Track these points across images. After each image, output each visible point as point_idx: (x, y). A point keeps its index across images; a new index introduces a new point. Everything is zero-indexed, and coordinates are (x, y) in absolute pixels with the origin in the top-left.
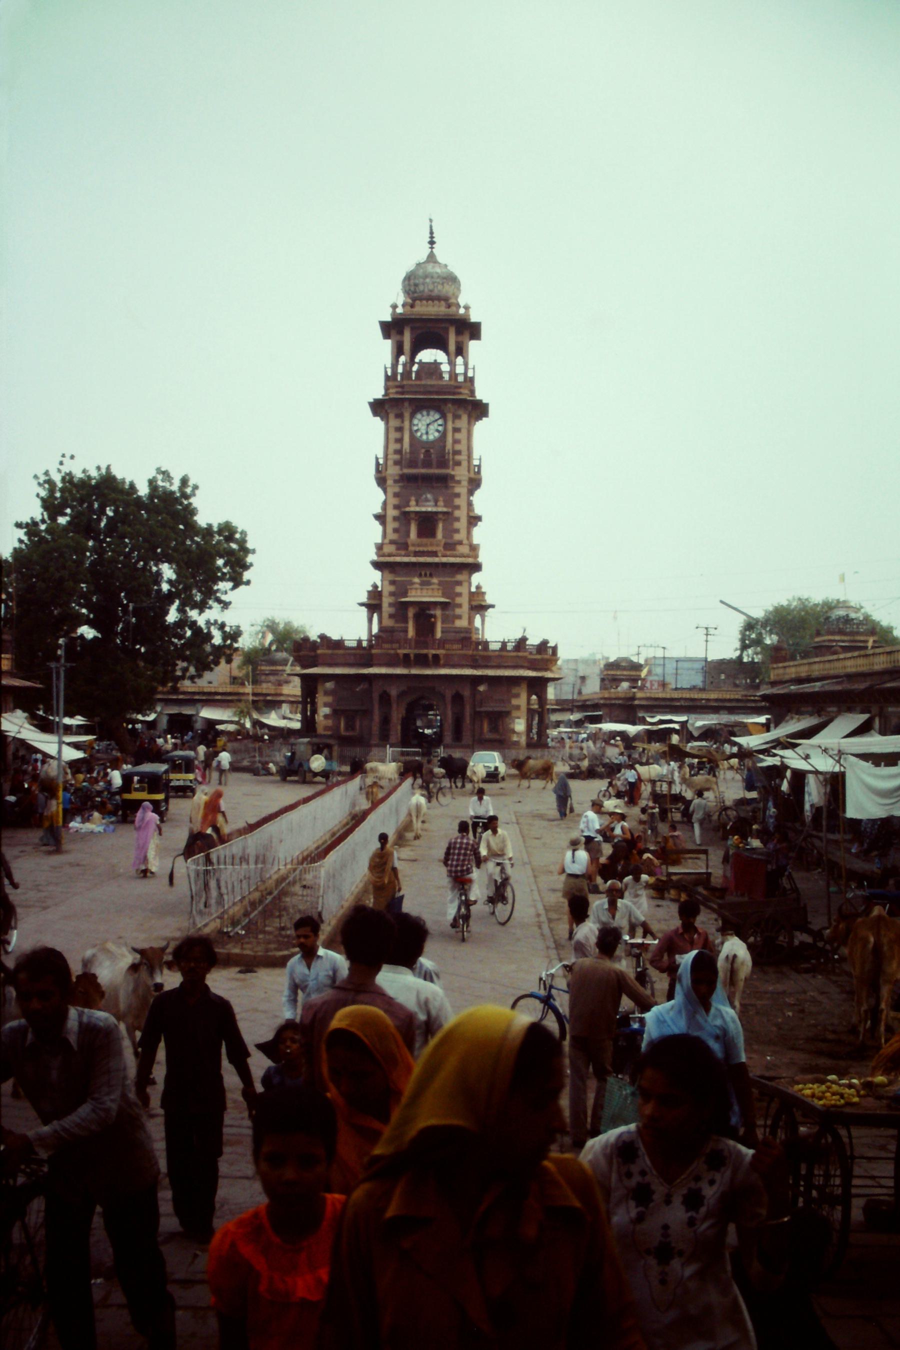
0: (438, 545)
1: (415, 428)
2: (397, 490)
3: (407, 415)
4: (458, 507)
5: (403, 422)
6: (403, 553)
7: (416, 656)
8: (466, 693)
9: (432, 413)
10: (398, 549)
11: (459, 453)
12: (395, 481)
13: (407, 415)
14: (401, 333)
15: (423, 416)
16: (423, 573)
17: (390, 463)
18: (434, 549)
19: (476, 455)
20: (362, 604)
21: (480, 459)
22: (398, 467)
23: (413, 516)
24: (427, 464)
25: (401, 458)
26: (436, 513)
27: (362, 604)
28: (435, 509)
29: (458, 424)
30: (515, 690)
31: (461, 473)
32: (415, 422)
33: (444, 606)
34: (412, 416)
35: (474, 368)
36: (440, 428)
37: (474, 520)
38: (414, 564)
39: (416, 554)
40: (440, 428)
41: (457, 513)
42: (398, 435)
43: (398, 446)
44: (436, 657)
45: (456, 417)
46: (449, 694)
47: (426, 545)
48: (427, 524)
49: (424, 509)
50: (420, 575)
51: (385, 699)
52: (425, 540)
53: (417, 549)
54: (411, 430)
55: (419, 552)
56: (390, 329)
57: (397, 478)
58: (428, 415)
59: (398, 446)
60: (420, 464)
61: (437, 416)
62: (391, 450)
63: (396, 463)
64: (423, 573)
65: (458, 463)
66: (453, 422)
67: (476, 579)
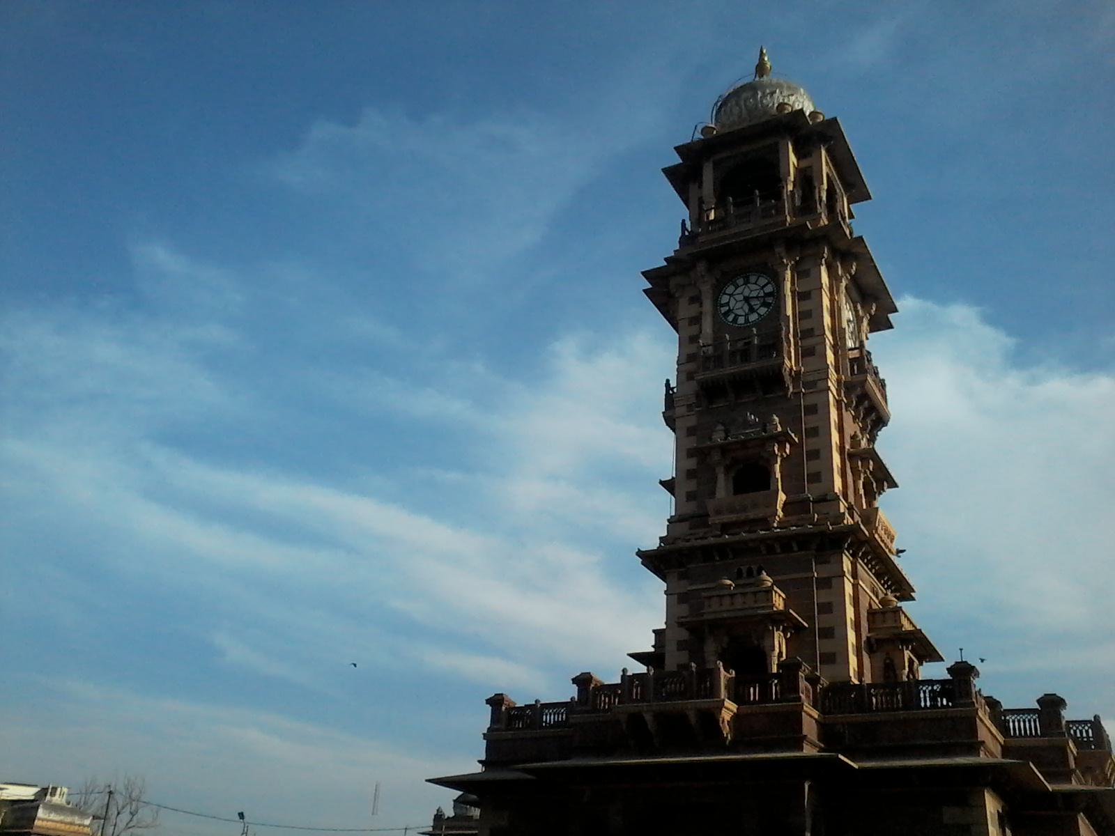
1: (724, 310)
3: (706, 289)
12: (690, 407)
15: (737, 287)
16: (744, 569)
23: (716, 456)
32: (725, 299)
34: (718, 291)
36: (770, 300)
38: (722, 550)
40: (770, 300)
47: (744, 509)
50: (739, 575)
54: (715, 315)
61: (763, 281)
64: (744, 569)
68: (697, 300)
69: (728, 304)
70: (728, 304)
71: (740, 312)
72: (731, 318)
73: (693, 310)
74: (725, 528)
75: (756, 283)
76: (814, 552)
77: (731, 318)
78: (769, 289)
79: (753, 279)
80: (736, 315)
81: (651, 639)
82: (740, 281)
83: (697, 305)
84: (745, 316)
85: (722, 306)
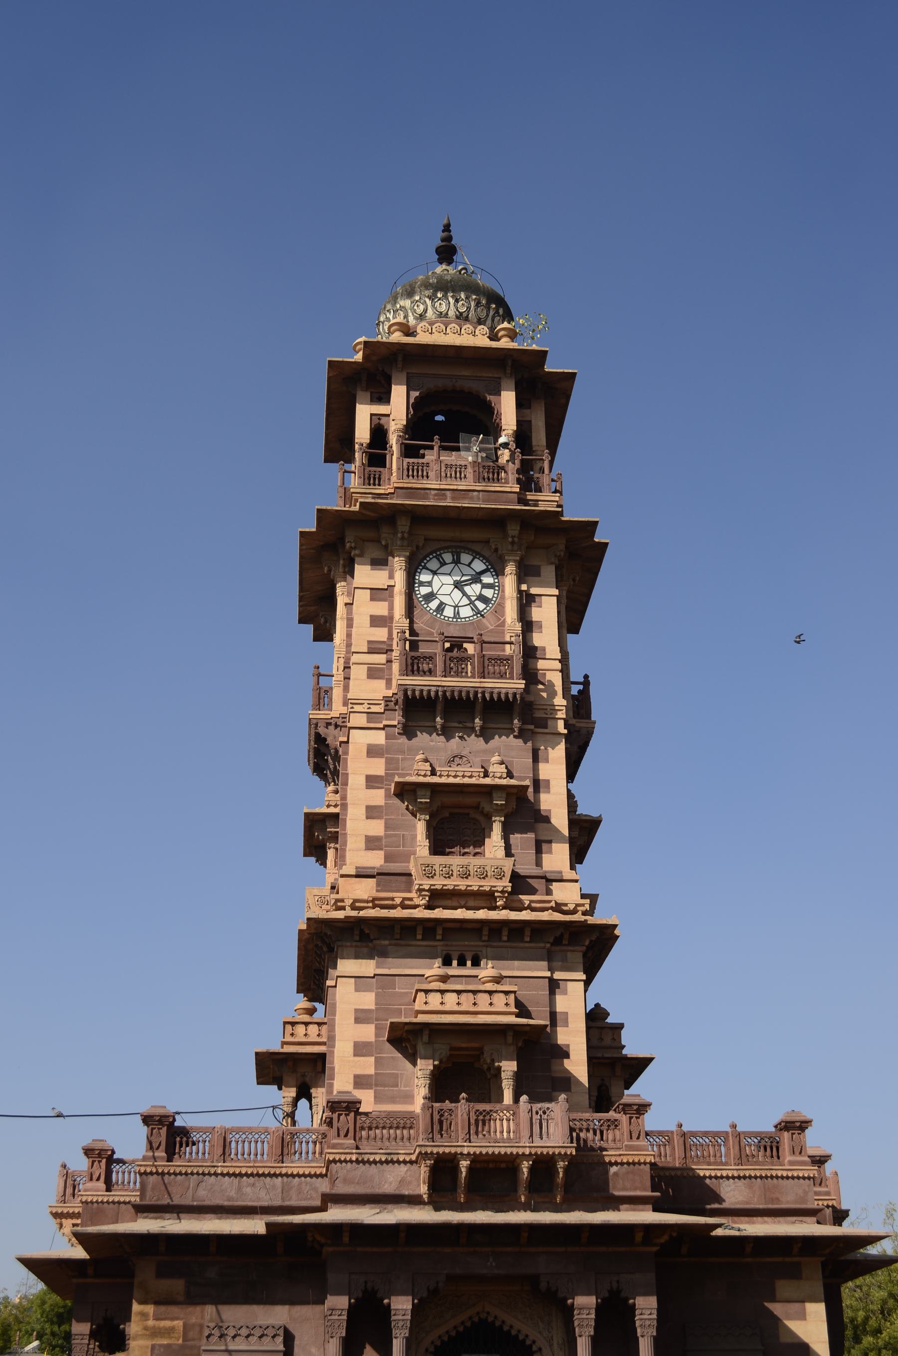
1: (424, 590)
2: (379, 738)
5: (391, 577)
6: (398, 896)
9: (465, 558)
10: (380, 887)
14: (383, 397)
15: (443, 564)
17: (358, 673)
18: (486, 885)
19: (576, 675)
21: (586, 682)
22: (380, 684)
25: (389, 661)
37: (583, 832)
38: (430, 927)
40: (488, 593)
42: (381, 609)
44: (543, 1165)
52: (455, 861)
53: (439, 883)
57: (379, 709)
58: (457, 562)
59: (381, 634)
62: (360, 644)
63: (373, 673)
66: (520, 581)
69: (430, 584)
70: (430, 584)
71: (446, 599)
72: (434, 605)
74: (437, 897)
75: (469, 565)
76: (548, 945)
77: (434, 605)
79: (465, 558)
80: (442, 603)
82: (448, 557)
84: (455, 607)
85: (422, 584)
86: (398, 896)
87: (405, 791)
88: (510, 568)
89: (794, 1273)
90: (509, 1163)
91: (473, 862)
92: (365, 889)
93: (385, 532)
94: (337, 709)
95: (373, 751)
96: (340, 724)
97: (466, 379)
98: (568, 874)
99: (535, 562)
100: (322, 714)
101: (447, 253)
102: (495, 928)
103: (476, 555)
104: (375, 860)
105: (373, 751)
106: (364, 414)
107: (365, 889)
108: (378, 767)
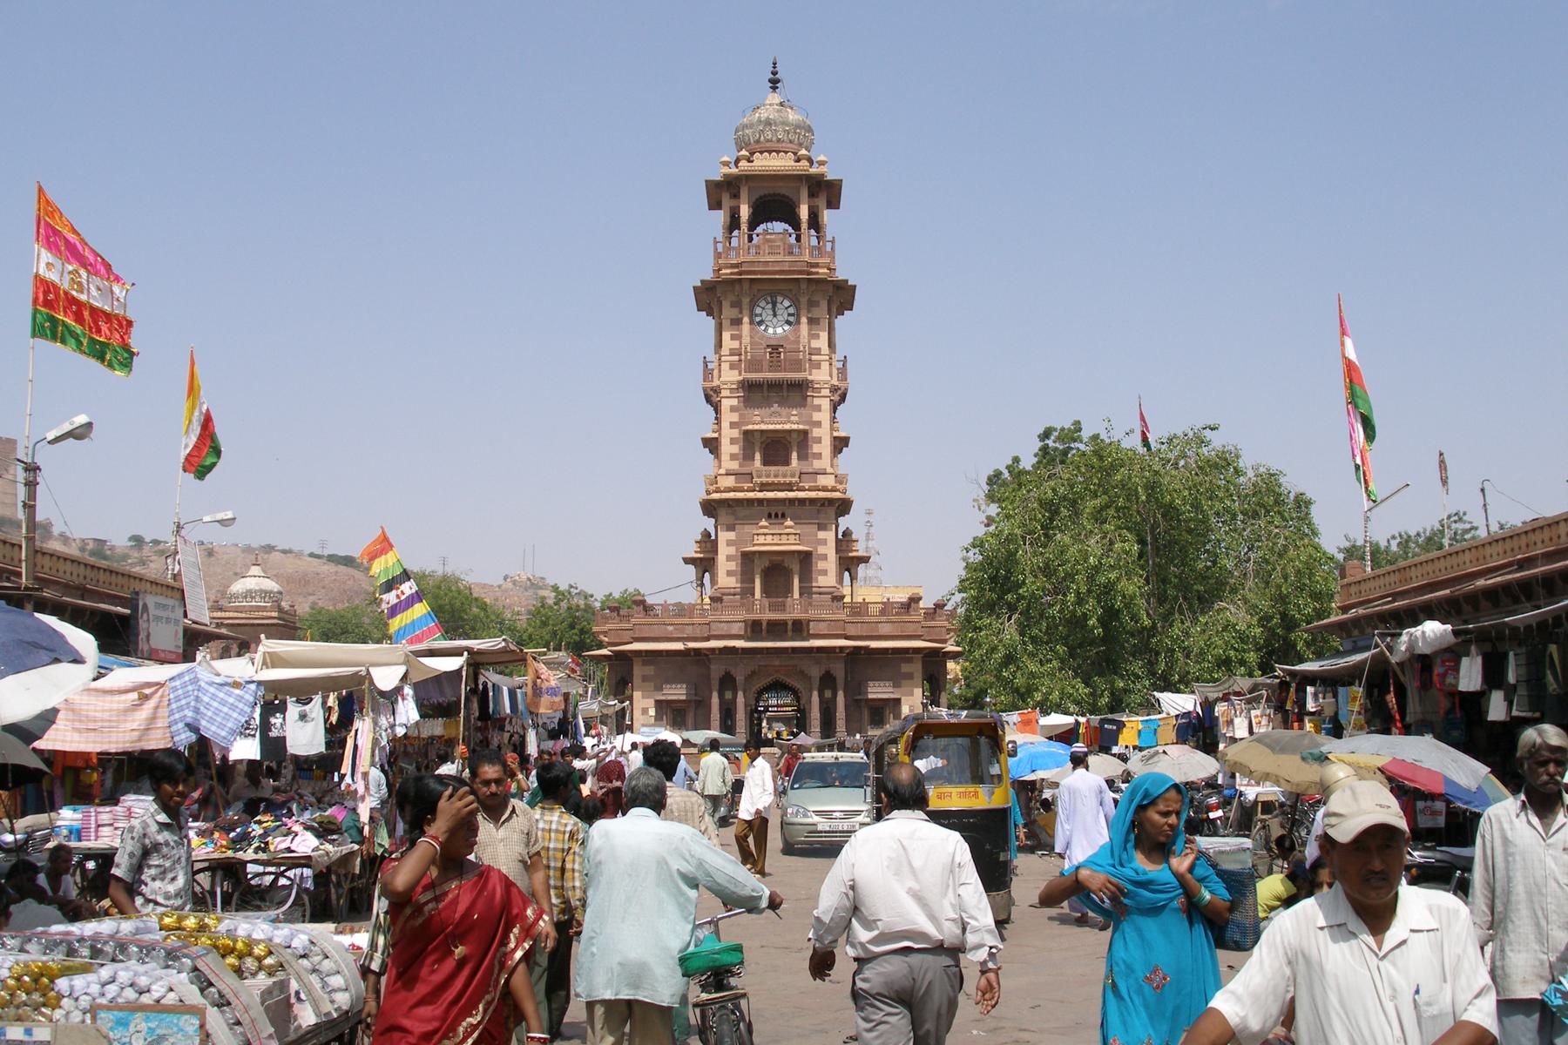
0: (793, 476)
2: (735, 402)
3: (746, 300)
4: (819, 424)
6: (746, 486)
7: (771, 623)
8: (839, 671)
11: (818, 351)
13: (746, 300)
14: (736, 196)
17: (725, 366)
18: (788, 480)
20: (687, 561)
24: (775, 365)
26: (790, 432)
27: (687, 561)
28: (787, 427)
29: (816, 313)
30: (905, 668)
31: (822, 375)
32: (758, 310)
33: (806, 559)
35: (833, 242)
36: (791, 319)
38: (760, 501)
39: (764, 487)
40: (791, 319)
41: (816, 432)
43: (736, 344)
45: (812, 304)
46: (815, 672)
48: (776, 448)
49: (771, 427)
50: (770, 516)
51: (727, 682)
52: (773, 469)
53: (764, 480)
55: (768, 484)
56: (721, 191)
59: (736, 344)
60: (766, 365)
61: (786, 303)
63: (732, 367)
65: (818, 366)
67: (844, 522)
68: (737, 304)
73: (734, 313)
78: (791, 310)
81: (695, 547)
83: (736, 310)
86: (746, 486)
87: (747, 434)
88: (804, 305)
89: (910, 661)
90: (784, 623)
91: (782, 469)
92: (730, 482)
93: (737, 287)
94: (716, 383)
95: (733, 409)
96: (717, 390)
97: (783, 189)
98: (829, 470)
99: (816, 298)
100: (708, 385)
101: (774, 83)
102: (792, 501)
103: (785, 297)
104: (734, 465)
105: (733, 409)
106: (727, 202)
107: (730, 482)
108: (735, 417)
